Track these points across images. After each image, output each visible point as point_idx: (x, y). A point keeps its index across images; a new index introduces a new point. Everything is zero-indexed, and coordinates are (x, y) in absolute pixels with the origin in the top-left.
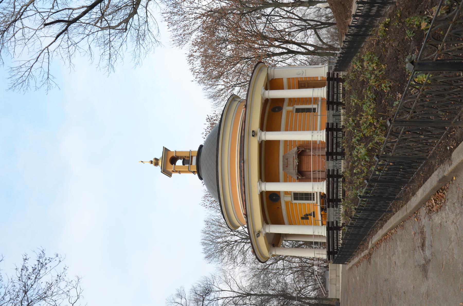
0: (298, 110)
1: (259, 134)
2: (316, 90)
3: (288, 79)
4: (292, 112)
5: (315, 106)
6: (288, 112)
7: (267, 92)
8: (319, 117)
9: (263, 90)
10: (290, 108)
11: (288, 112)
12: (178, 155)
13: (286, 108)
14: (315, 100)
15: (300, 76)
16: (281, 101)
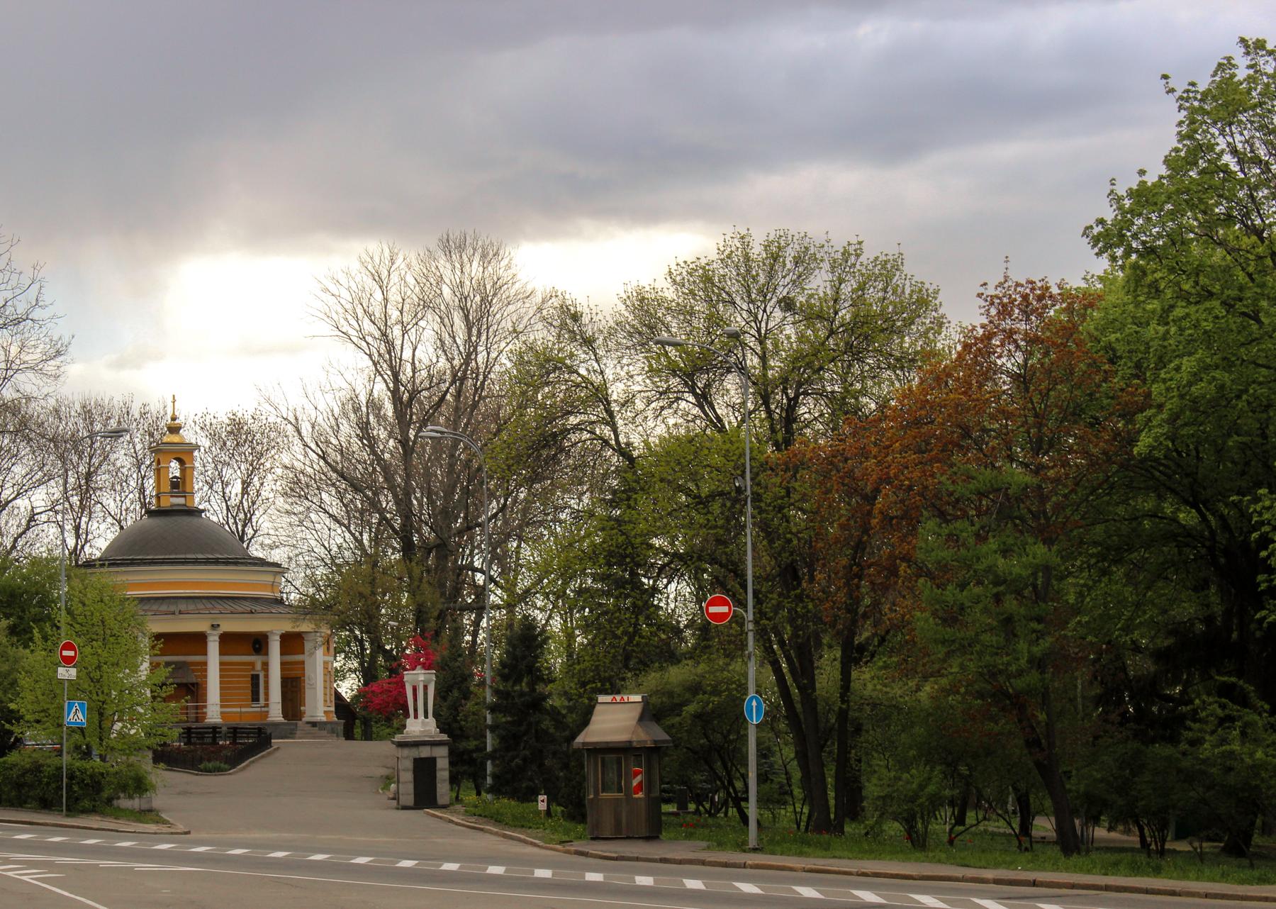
0: (255, 679)
1: (215, 632)
2: (280, 706)
3: (303, 663)
4: (253, 669)
5: (262, 701)
6: (252, 664)
7: (278, 638)
8: (239, 710)
9: (280, 633)
10: (259, 666)
11: (252, 664)
12: (188, 471)
13: (257, 660)
14: (267, 705)
15: (307, 681)
16: (267, 654)
